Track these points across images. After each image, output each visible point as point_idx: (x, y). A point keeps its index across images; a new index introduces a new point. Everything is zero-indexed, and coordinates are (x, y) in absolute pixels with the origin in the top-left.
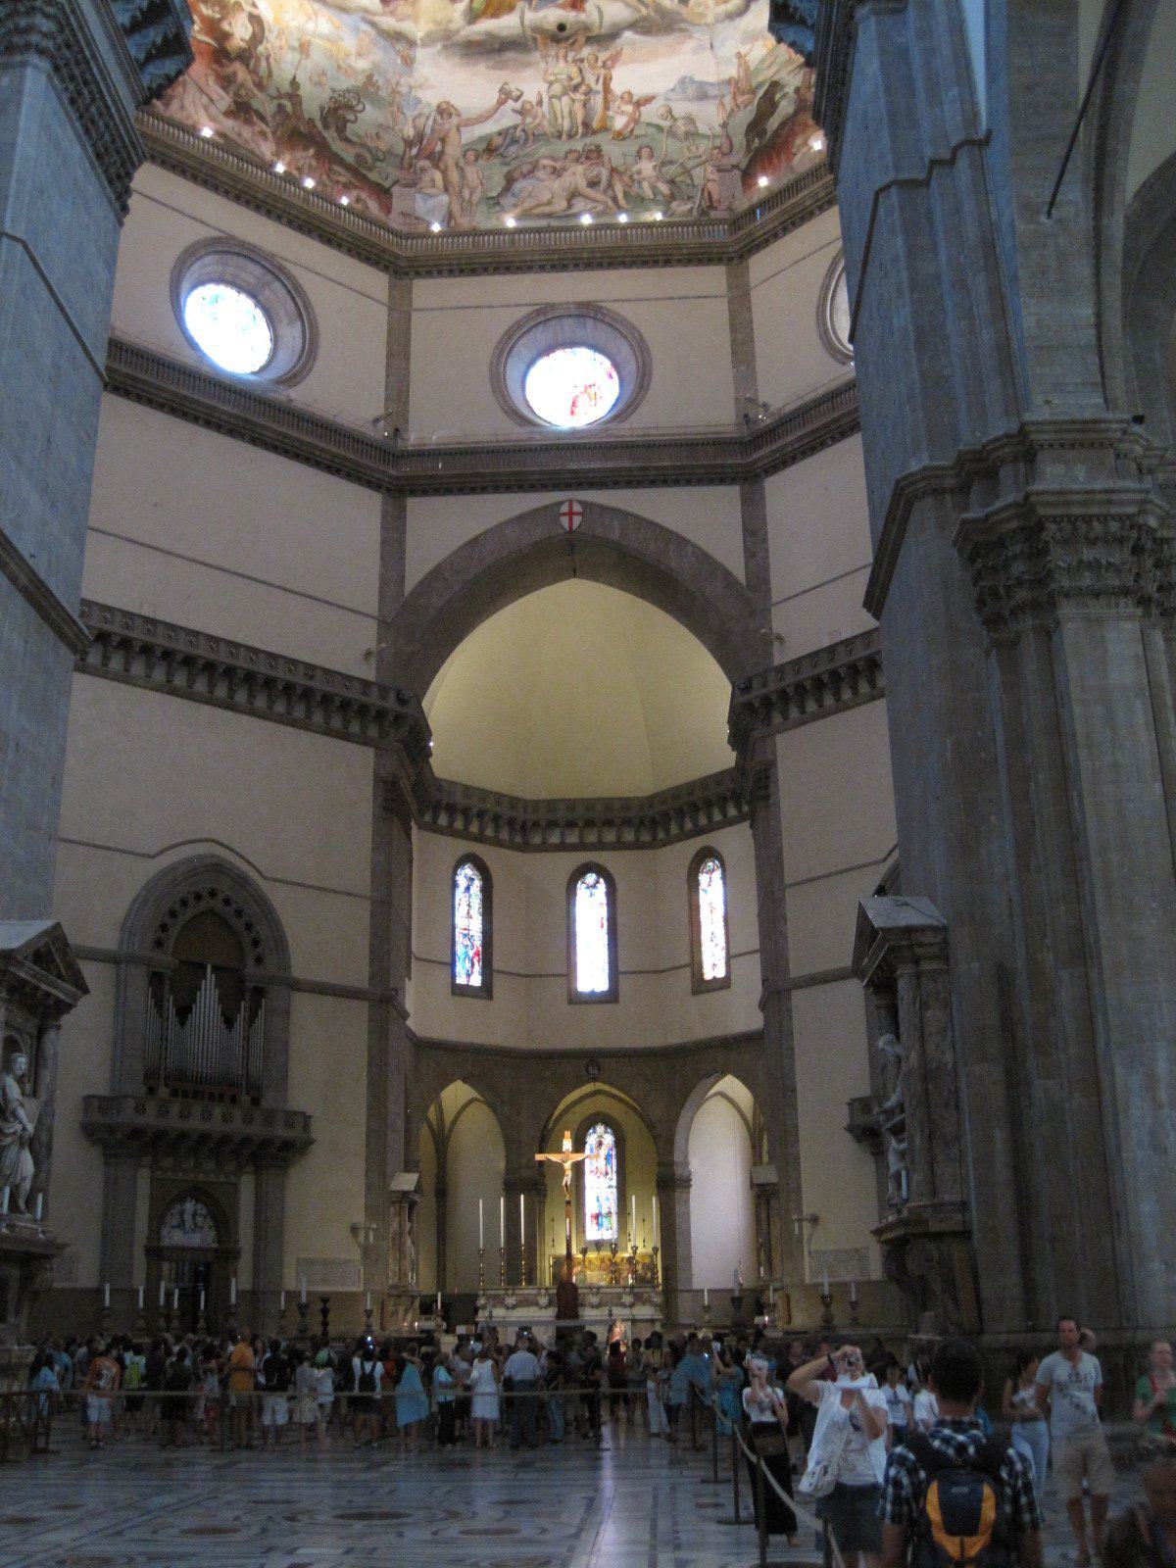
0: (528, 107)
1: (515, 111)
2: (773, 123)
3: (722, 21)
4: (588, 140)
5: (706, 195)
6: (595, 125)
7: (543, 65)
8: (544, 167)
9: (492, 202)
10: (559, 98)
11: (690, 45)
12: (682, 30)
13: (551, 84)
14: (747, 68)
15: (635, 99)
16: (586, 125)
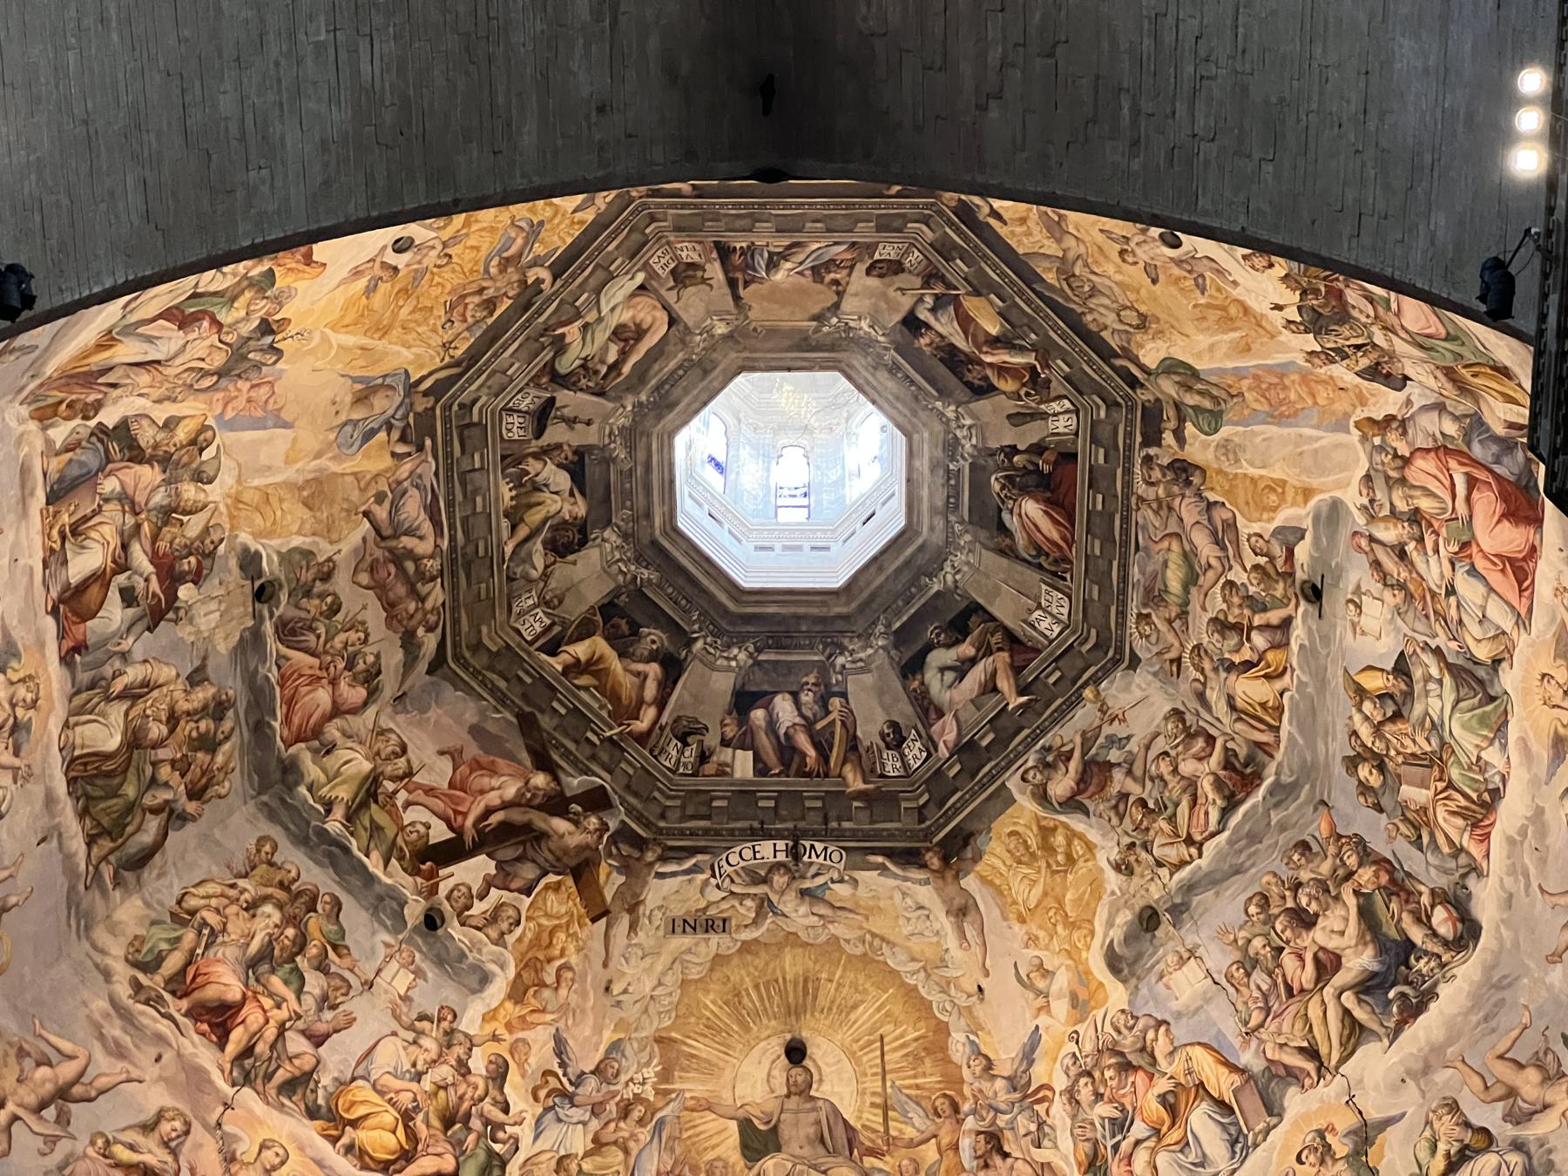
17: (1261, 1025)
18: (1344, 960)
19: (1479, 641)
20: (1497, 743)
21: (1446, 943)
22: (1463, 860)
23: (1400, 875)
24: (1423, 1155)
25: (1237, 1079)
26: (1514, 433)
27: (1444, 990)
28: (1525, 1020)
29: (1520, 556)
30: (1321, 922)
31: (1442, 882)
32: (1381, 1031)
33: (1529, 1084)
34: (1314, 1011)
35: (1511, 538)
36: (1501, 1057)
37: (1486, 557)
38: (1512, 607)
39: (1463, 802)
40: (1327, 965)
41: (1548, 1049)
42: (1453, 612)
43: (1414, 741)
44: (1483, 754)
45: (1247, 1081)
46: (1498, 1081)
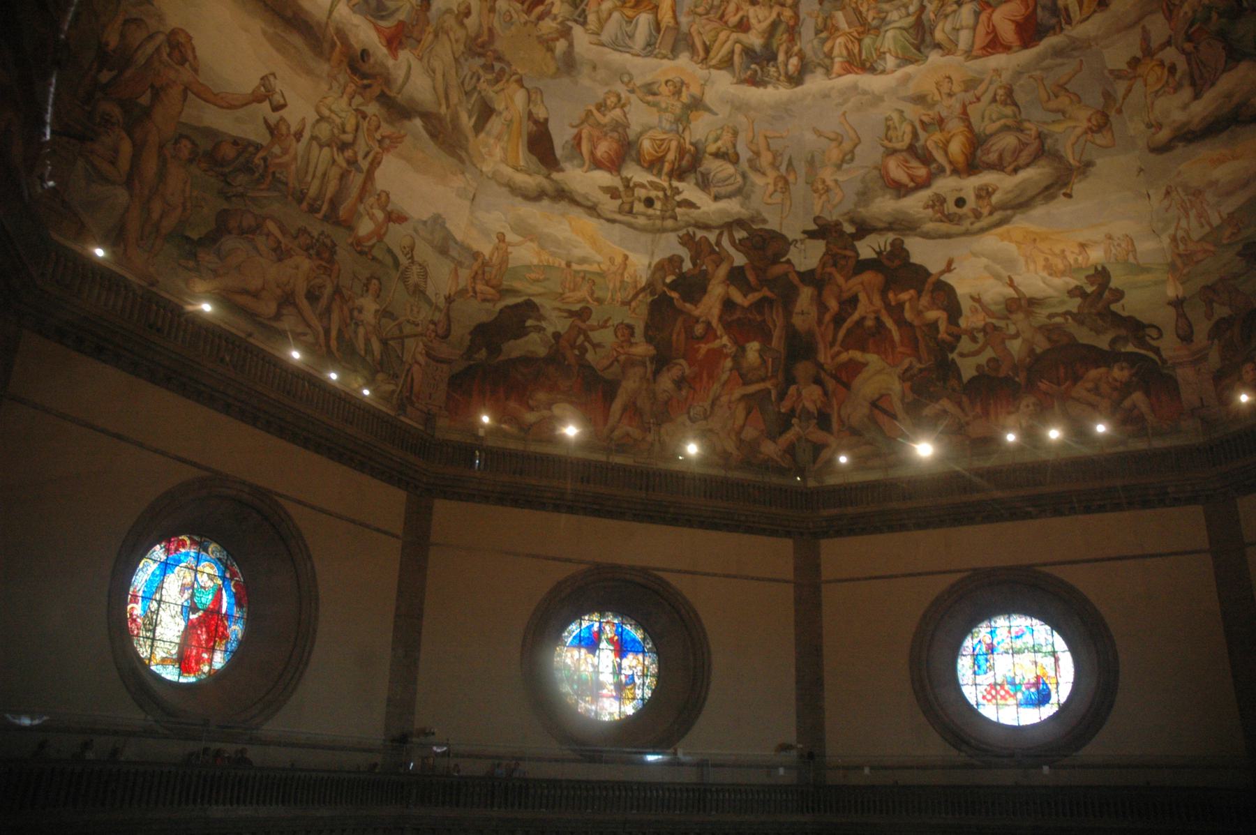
0: (284, 129)
1: (266, 121)
2: (515, 348)
3: (501, 184)
4: (328, 228)
5: (409, 379)
6: (342, 212)
7: (324, 86)
8: (269, 234)
9: (187, 247)
10: (321, 146)
11: (458, 182)
12: (461, 161)
13: (322, 118)
14: (504, 261)
15: (389, 208)
16: (334, 204)
17: (700, 15)
18: (750, 32)
19: (943, 31)
20: (898, 61)
21: (786, 73)
22: (827, 61)
23: (797, 29)
24: (711, 137)
25: (672, 23)
26: (1063, 12)
27: (770, 89)
28: (785, 134)
29: (1002, 42)
30: (757, 8)
31: (809, 53)
32: (737, 75)
33: (766, 158)
34: (723, 36)
35: (1008, 32)
36: (766, 137)
37: (989, 19)
38: (972, 46)
39: (856, 51)
40: (743, 26)
41: (781, 154)
42: (949, 9)
43: (868, 10)
44: (888, 56)
45: (675, 29)
46: (757, 144)
